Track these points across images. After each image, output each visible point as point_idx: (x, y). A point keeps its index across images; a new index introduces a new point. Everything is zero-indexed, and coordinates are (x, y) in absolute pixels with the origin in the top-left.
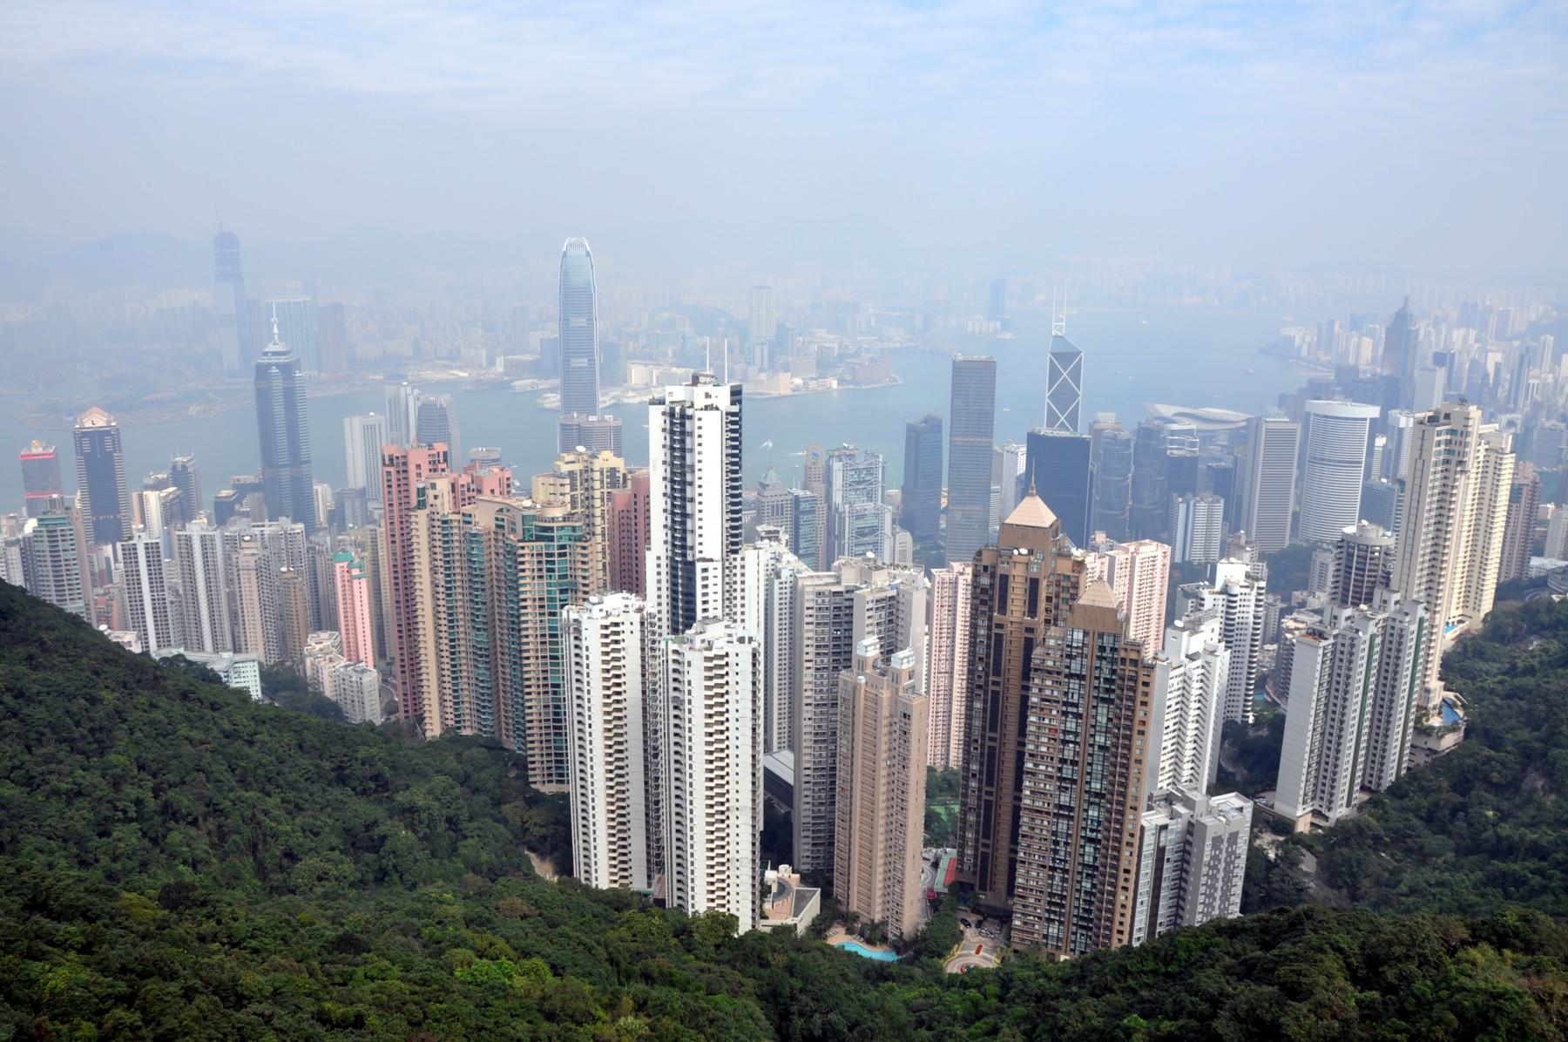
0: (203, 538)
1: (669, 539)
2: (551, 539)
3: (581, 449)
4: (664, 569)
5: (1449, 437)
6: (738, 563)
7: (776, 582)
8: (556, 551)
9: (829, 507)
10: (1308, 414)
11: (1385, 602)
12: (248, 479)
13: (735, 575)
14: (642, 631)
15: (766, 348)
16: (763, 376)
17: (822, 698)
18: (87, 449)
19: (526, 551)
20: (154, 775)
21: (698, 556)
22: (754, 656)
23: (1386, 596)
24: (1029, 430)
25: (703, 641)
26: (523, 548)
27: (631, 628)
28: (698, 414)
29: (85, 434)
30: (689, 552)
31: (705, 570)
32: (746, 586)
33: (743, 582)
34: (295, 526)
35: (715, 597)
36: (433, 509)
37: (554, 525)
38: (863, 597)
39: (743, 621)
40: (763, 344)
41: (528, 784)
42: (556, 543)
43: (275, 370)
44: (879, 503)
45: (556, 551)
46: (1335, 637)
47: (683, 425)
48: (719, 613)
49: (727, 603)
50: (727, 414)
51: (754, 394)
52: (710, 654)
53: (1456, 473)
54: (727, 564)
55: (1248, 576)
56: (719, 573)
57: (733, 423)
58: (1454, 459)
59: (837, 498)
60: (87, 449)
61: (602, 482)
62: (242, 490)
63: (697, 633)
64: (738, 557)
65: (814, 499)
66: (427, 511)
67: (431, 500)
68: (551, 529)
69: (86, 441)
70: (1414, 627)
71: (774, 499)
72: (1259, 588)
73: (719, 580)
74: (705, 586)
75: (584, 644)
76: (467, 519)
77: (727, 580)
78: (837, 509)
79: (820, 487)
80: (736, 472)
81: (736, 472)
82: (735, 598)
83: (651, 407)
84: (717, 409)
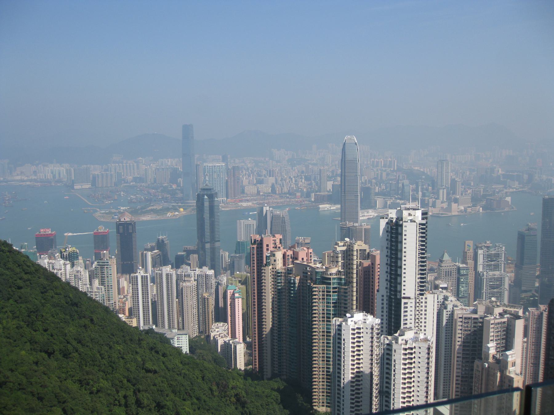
0: (167, 275)
1: (388, 286)
2: (330, 284)
3: (347, 239)
4: (385, 302)
6: (423, 300)
7: (445, 311)
8: (332, 290)
9: (476, 273)
12: (191, 247)
13: (422, 306)
14: (372, 333)
15: (445, 191)
17: (465, 374)
18: (121, 231)
19: (317, 289)
20: (134, 385)
21: (403, 296)
22: (429, 349)
25: (402, 340)
26: (316, 287)
27: (367, 331)
28: (404, 224)
29: (121, 224)
30: (398, 294)
31: (405, 303)
32: (427, 313)
33: (426, 310)
34: (210, 271)
35: (411, 317)
36: (274, 266)
37: (332, 277)
38: (489, 321)
39: (425, 330)
41: (312, 406)
42: (332, 286)
43: (206, 197)
44: (502, 272)
45: (332, 290)
47: (397, 229)
48: (412, 325)
49: (417, 321)
50: (420, 224)
52: (407, 346)
54: (418, 301)
56: (413, 305)
57: (422, 229)
59: (480, 269)
60: (121, 231)
61: (357, 257)
62: (189, 252)
63: (400, 335)
64: (424, 297)
65: (467, 269)
66: (271, 267)
67: (272, 262)
68: (330, 279)
69: (121, 227)
71: (446, 268)
73: (413, 309)
74: (406, 311)
75: (343, 337)
76: (289, 272)
77: (417, 309)
79: (471, 262)
80: (423, 254)
81: (423, 254)
82: (421, 318)
83: (381, 220)
84: (415, 222)
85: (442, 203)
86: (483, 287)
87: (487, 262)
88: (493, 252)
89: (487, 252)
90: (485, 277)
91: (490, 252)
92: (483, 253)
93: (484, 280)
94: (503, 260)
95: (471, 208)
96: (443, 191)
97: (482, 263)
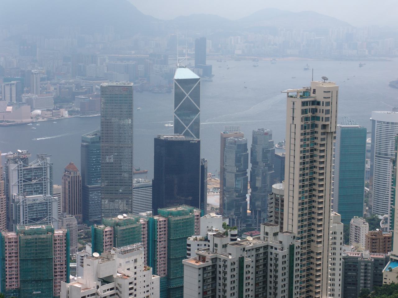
5: (314, 107)
9: (8, 198)
10: (373, 121)
11: (267, 234)
15: (14, 88)
16: (9, 109)
23: (268, 229)
24: (156, 137)
40: (11, 84)
46: (214, 260)
51: (3, 121)
53: (323, 134)
55: (224, 226)
58: (320, 123)
59: (14, 192)
70: (286, 251)
72: (232, 235)
78: (14, 200)
85: (8, 106)
86: (19, 218)
87: (24, 181)
88: (33, 167)
89: (24, 166)
90: (22, 204)
91: (29, 167)
92: (17, 168)
93: (19, 208)
94: (49, 177)
95: (51, 113)
96: (11, 89)
97: (17, 184)
